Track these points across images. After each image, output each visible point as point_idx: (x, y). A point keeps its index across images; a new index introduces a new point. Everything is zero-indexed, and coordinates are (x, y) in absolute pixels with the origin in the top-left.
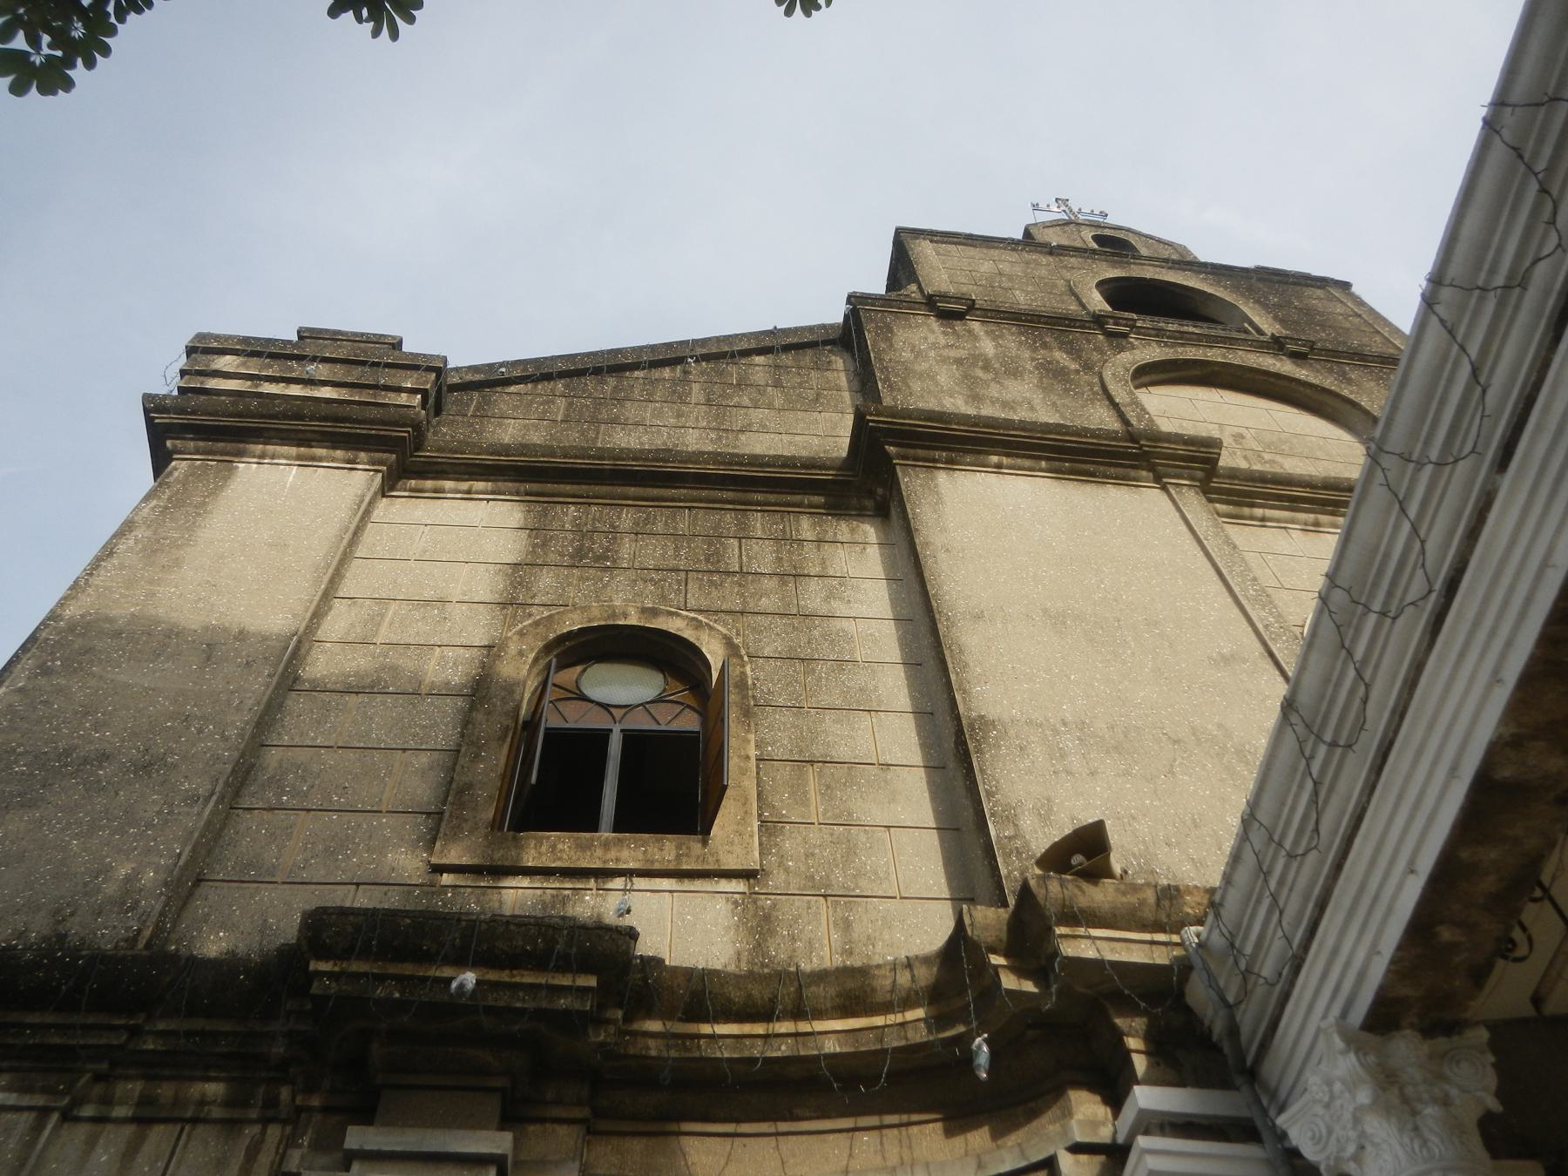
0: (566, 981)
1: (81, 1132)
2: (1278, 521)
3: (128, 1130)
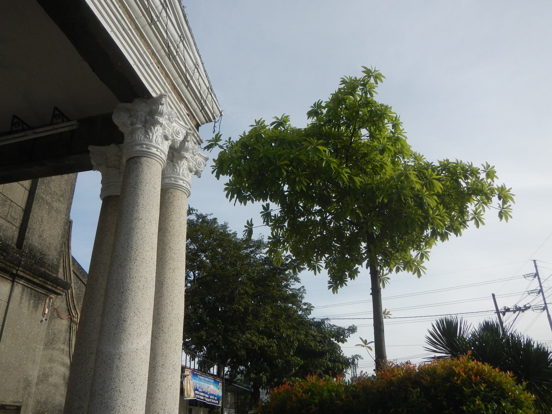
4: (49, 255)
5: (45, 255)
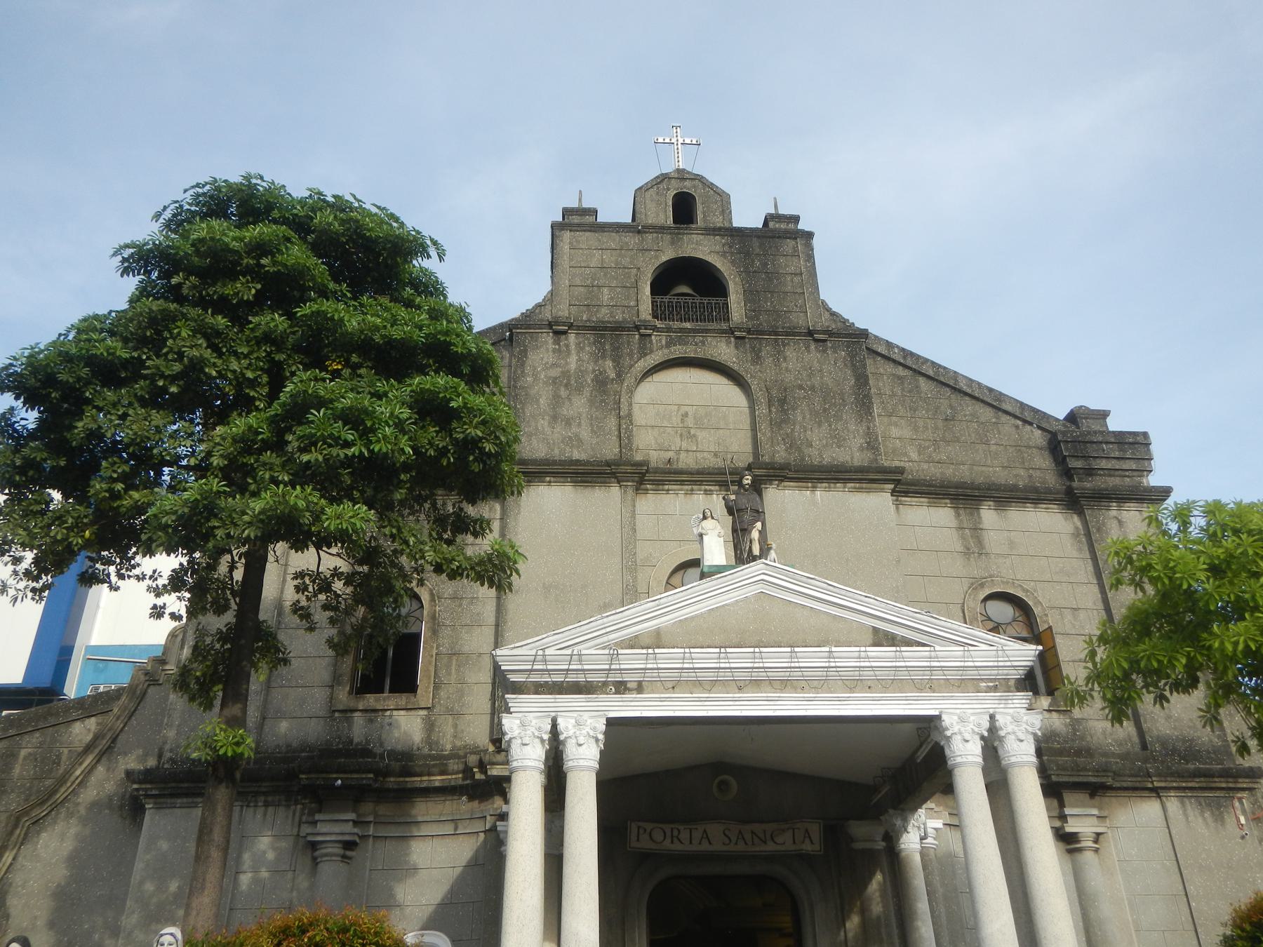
0: (364, 776)
1: (251, 810)
2: (675, 490)
3: (263, 808)
4: (1199, 738)
5: (1192, 740)
